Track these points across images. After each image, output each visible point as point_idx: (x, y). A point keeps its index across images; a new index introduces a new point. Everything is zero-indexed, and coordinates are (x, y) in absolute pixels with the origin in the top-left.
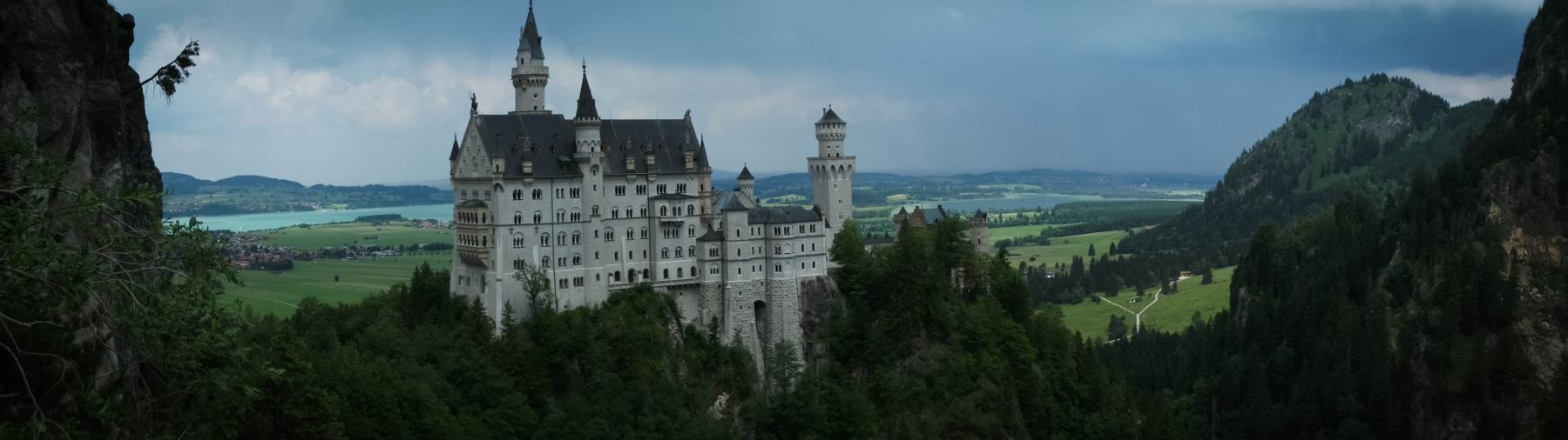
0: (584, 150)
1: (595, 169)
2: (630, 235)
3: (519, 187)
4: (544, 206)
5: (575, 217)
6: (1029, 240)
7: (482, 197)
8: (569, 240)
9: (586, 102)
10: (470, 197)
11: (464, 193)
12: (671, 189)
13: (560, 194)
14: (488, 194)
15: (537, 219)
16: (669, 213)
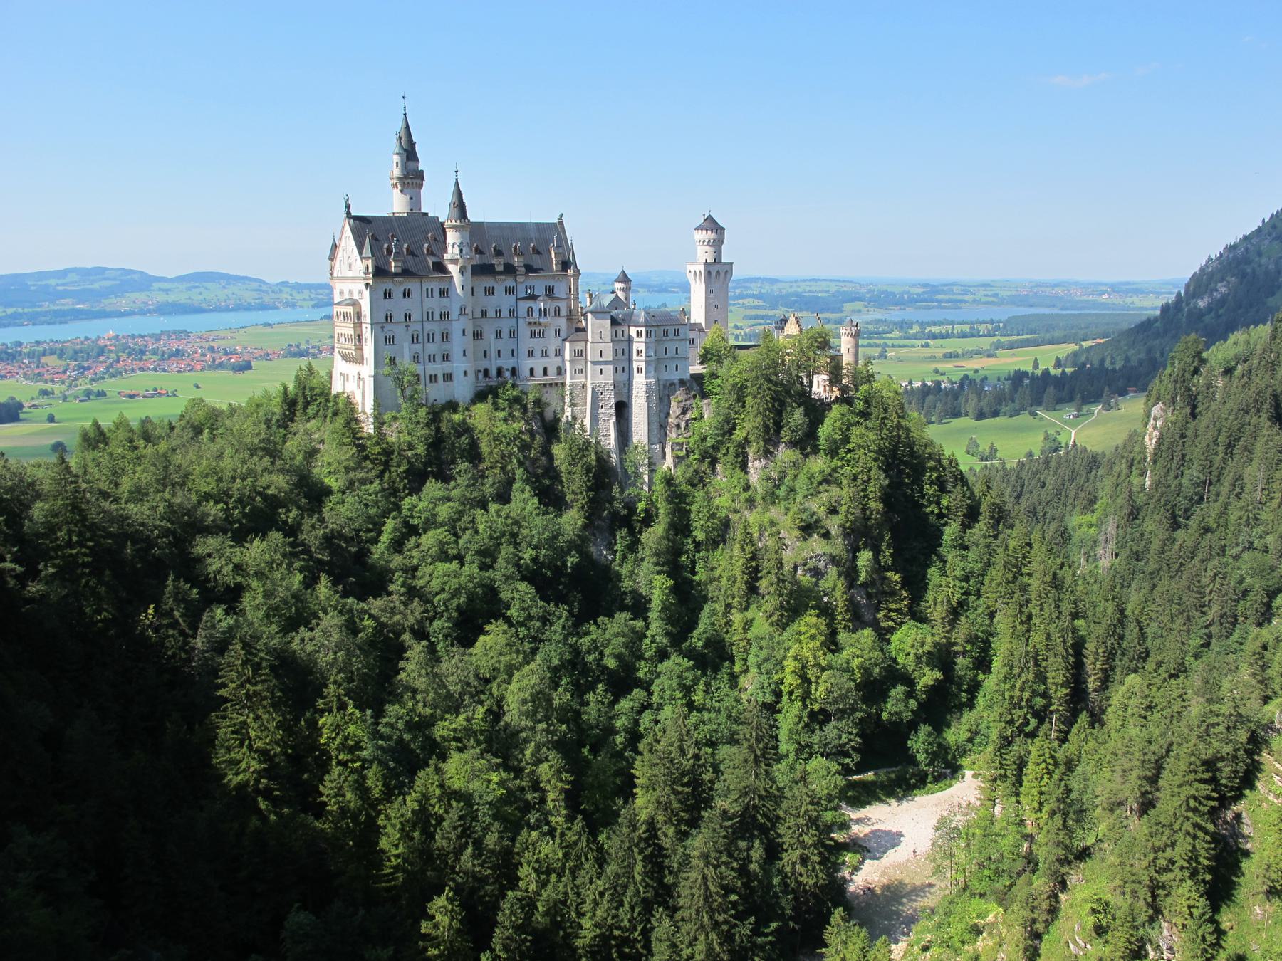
0: (452, 252)
1: (462, 272)
2: (498, 334)
3: (387, 284)
4: (412, 305)
5: (444, 316)
6: (978, 353)
7: (356, 296)
8: (438, 338)
9: (460, 207)
10: (347, 296)
11: (342, 293)
12: (540, 290)
13: (429, 293)
14: (361, 293)
15: (408, 317)
16: (536, 314)
